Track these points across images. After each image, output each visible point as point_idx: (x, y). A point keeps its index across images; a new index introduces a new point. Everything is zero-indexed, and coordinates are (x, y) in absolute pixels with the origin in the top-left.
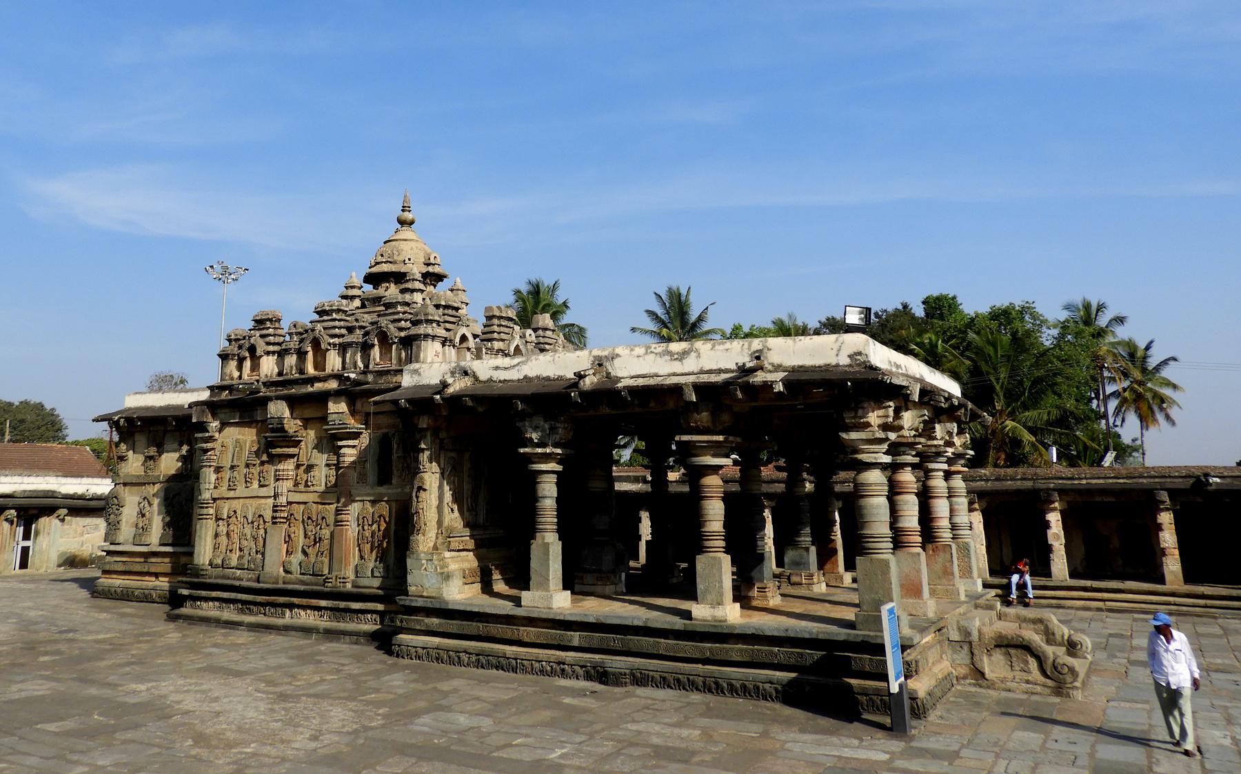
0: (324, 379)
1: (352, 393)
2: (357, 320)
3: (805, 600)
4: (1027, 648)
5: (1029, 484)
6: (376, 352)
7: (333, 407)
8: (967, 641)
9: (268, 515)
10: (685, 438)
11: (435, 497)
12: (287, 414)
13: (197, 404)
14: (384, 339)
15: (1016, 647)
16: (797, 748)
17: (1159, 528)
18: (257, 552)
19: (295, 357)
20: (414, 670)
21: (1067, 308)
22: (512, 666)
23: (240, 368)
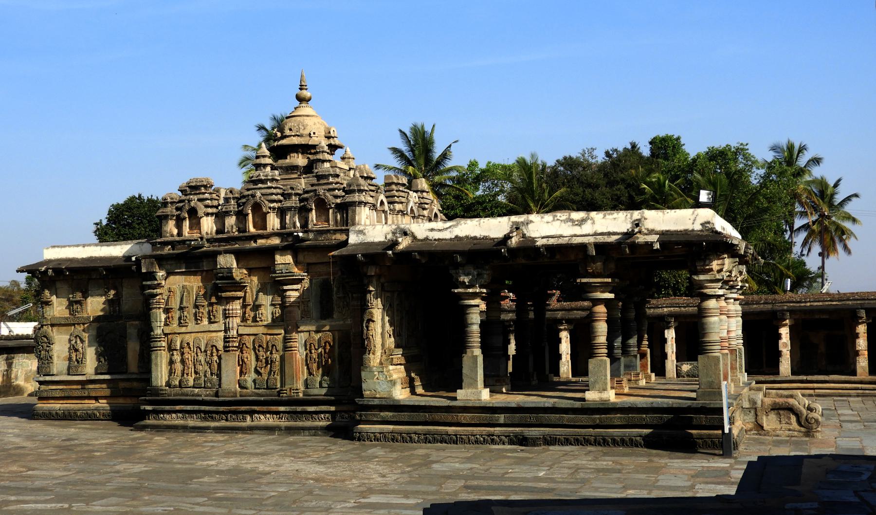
0: (268, 236)
1: (293, 245)
2: (292, 188)
3: (668, 385)
4: (791, 409)
5: (770, 306)
6: (313, 215)
7: (279, 259)
8: (754, 408)
9: (220, 345)
10: (584, 280)
11: (380, 327)
12: (235, 265)
13: (145, 257)
14: (322, 206)
15: (784, 409)
16: (675, 465)
17: (857, 336)
18: (212, 374)
19: (234, 218)
20: (383, 447)
21: (774, 149)
22: (455, 440)
23: (179, 226)
